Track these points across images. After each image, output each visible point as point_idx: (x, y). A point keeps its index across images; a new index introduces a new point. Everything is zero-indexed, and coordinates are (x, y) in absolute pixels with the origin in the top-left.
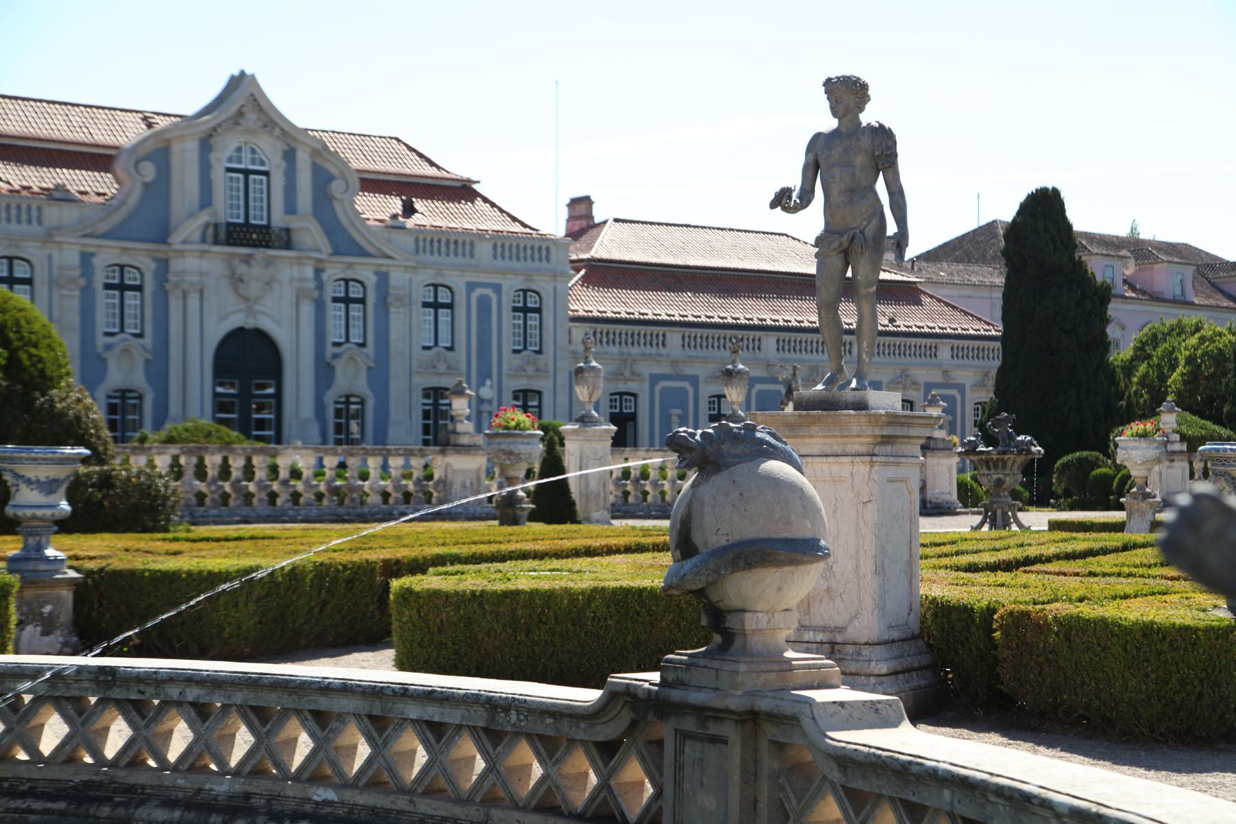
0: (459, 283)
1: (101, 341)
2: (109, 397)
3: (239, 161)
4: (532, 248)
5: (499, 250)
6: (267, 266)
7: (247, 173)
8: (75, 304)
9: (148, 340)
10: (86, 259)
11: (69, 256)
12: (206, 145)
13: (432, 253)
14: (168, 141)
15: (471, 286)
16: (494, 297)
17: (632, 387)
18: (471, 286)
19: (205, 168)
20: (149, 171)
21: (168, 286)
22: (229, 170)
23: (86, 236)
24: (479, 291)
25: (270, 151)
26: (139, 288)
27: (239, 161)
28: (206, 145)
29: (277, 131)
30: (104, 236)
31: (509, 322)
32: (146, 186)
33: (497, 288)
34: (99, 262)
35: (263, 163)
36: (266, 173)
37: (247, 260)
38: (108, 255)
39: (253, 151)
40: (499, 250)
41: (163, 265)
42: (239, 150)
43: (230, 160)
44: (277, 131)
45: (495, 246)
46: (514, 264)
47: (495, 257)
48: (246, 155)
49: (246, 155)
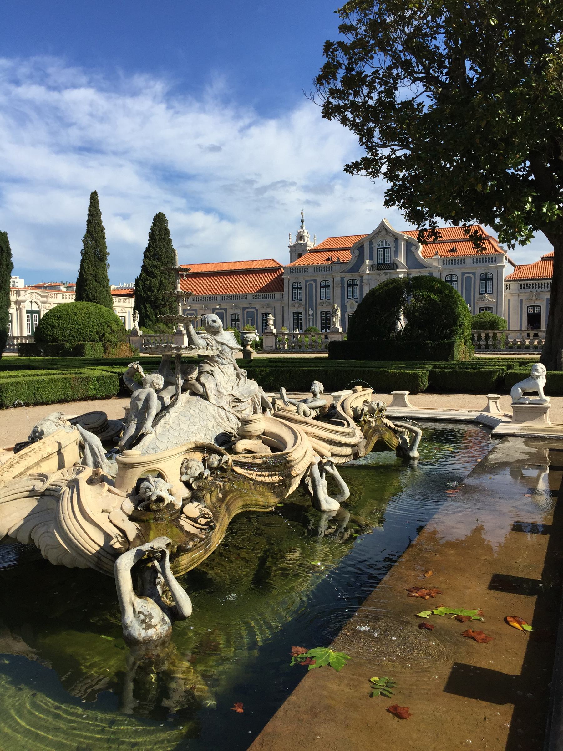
0: (458, 273)
1: (346, 300)
2: (349, 316)
3: (382, 245)
4: (489, 258)
5: (475, 260)
6: (385, 275)
7: (384, 248)
8: (339, 291)
9: (358, 300)
10: (342, 279)
11: (338, 279)
12: (371, 243)
13: (455, 264)
14: (362, 243)
15: (463, 274)
16: (472, 277)
17: (537, 303)
18: (463, 274)
19: (371, 249)
20: (357, 253)
21: (363, 284)
22: (378, 249)
23: (341, 272)
24: (466, 275)
25: (390, 241)
26: (456, 281)
27: (382, 245)
28: (371, 243)
29: (391, 235)
30: (347, 272)
31: (477, 285)
32: (359, 256)
33: (474, 274)
34: (346, 280)
35: (389, 245)
36: (390, 248)
37: (379, 274)
38: (348, 276)
39: (386, 242)
40: (475, 260)
41: (362, 277)
42: (382, 242)
43: (379, 245)
44: (391, 235)
45: (474, 259)
46: (481, 265)
47: (473, 263)
48: (384, 243)
49: (384, 243)
